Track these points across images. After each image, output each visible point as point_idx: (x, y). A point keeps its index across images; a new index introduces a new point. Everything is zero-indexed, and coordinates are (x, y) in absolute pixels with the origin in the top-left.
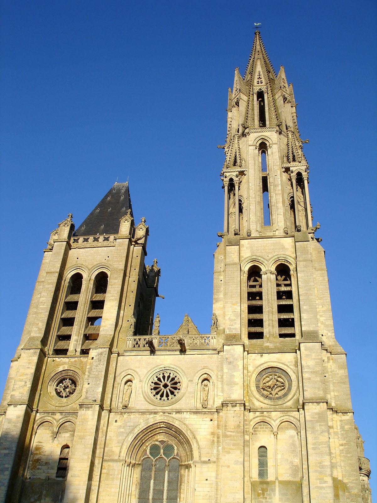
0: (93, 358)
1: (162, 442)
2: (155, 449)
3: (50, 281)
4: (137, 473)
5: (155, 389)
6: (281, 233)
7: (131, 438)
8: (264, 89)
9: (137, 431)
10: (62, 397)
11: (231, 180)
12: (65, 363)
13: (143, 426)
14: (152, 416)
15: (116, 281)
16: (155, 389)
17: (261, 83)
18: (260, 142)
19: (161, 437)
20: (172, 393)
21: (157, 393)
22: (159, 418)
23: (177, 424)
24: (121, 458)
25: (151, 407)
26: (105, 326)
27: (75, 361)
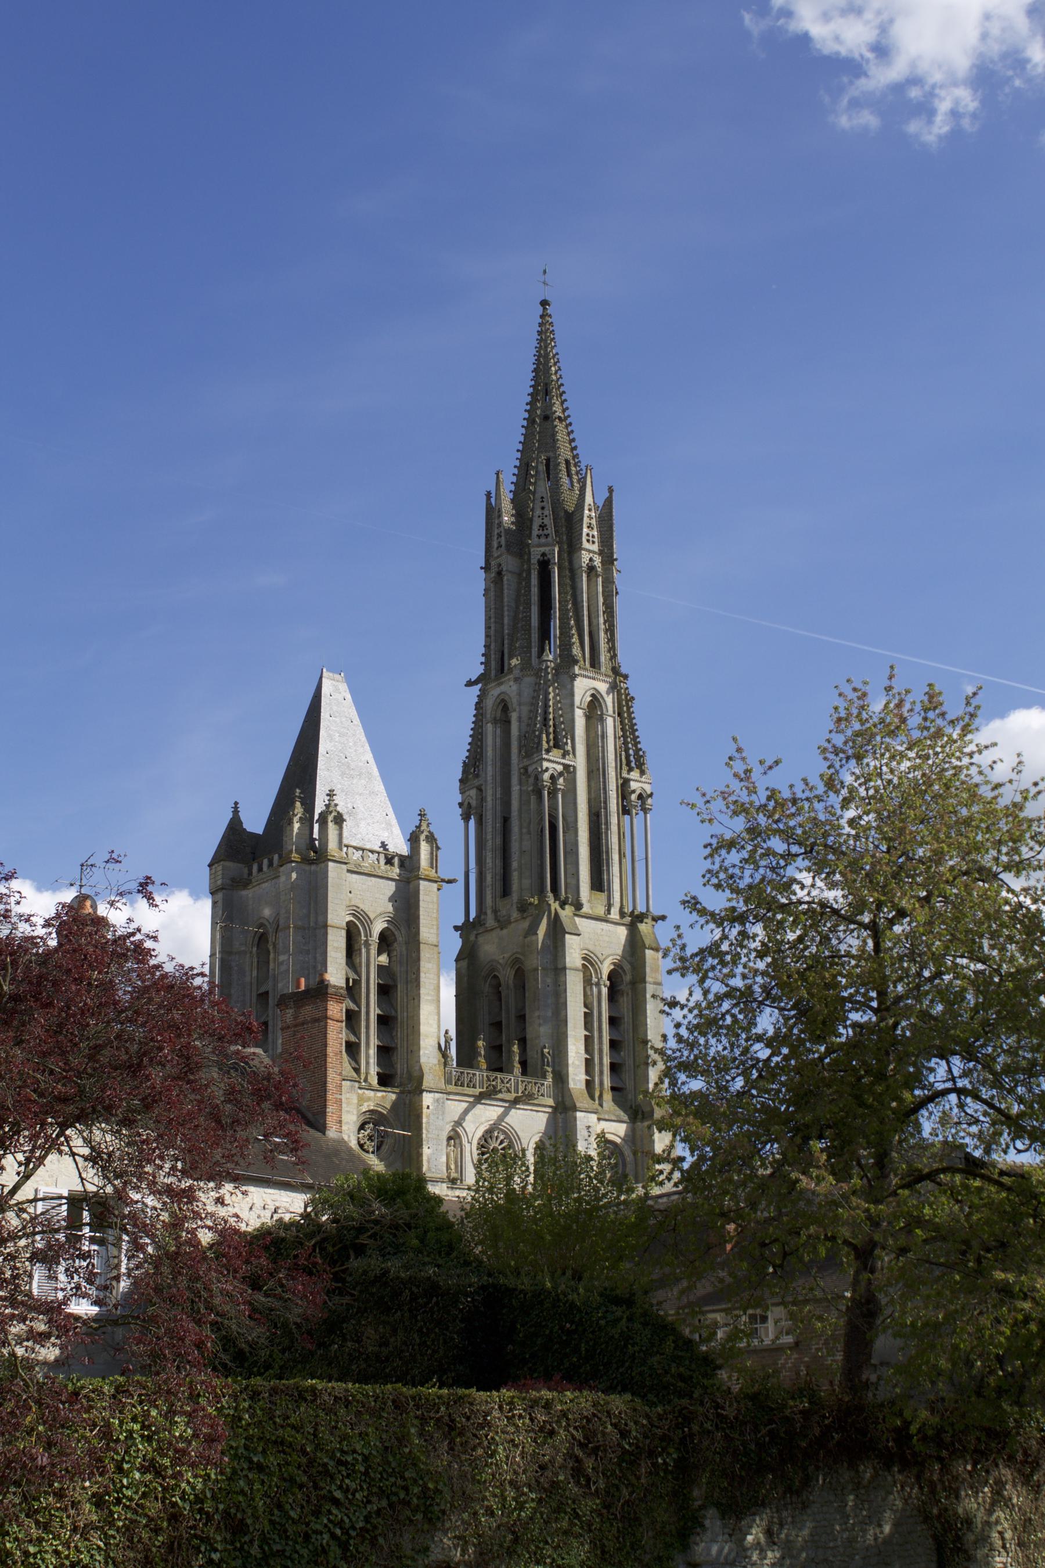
0: (428, 1107)
3: (335, 945)
6: (615, 915)
10: (368, 1152)
12: (369, 1099)
15: (430, 965)
17: (593, 542)
26: (426, 1048)
27: (383, 1097)
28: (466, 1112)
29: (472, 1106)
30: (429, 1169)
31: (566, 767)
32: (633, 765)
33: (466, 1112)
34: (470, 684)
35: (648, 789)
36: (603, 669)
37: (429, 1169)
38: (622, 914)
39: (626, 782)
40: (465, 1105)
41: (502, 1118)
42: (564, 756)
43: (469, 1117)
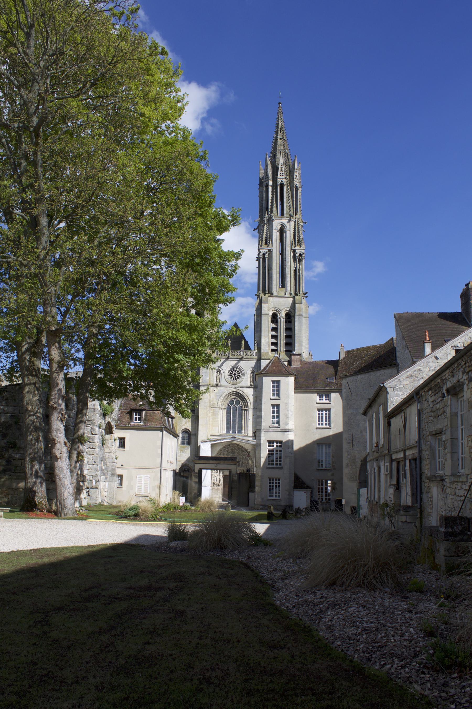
1: (235, 399)
2: (232, 402)
4: (225, 412)
5: (230, 376)
6: (288, 294)
7: (222, 398)
8: (284, 181)
9: (224, 395)
11: (264, 254)
13: (227, 393)
14: (230, 388)
16: (230, 376)
18: (280, 226)
19: (233, 397)
20: (238, 378)
21: (231, 378)
22: (233, 390)
23: (241, 392)
24: (218, 406)
25: (229, 385)
28: (223, 363)
29: (225, 361)
30: (202, 382)
31: (269, 250)
32: (297, 244)
33: (223, 363)
34: (255, 230)
35: (303, 251)
36: (285, 215)
37: (202, 382)
38: (291, 294)
39: (294, 251)
40: (222, 361)
41: (237, 364)
42: (268, 247)
43: (224, 365)
